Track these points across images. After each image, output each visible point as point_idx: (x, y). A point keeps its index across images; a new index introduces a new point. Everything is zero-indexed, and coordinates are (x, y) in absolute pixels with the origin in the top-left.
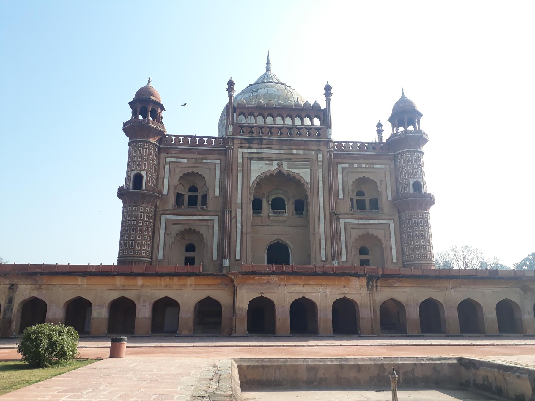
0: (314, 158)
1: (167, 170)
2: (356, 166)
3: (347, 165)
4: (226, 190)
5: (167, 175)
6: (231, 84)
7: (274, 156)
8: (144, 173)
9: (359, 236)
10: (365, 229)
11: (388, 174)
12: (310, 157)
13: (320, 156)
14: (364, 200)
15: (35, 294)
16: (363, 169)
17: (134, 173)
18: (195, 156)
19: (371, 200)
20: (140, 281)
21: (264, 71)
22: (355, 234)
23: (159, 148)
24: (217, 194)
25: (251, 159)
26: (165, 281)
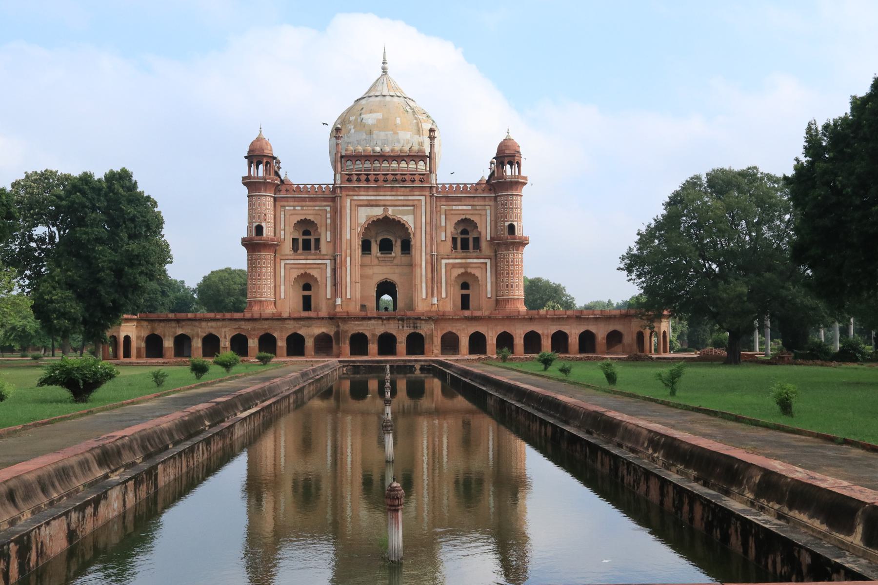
8: (263, 224)
21: (380, 72)
23: (275, 199)
24: (329, 239)
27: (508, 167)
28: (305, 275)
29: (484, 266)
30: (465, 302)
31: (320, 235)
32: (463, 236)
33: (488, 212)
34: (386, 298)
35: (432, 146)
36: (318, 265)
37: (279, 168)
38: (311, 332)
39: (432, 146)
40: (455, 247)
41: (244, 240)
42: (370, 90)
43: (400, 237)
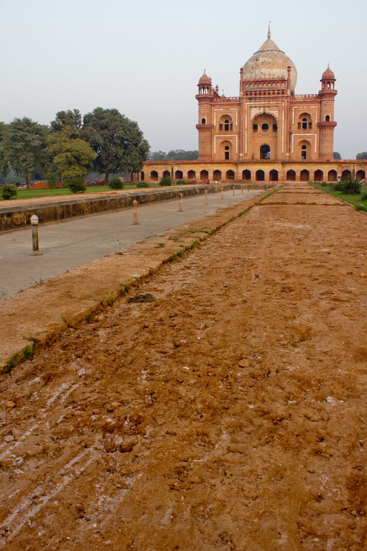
0: (280, 105)
1: (215, 115)
2: (301, 107)
3: (297, 107)
4: (240, 122)
5: (215, 117)
6: (242, 70)
7: (261, 105)
8: (206, 118)
11: (317, 111)
12: (278, 105)
13: (283, 104)
15: (179, 169)
16: (303, 109)
17: (202, 118)
18: (227, 107)
20: (209, 165)
22: (299, 140)
24: (237, 124)
25: (251, 107)
26: (216, 165)
36: (233, 137)
37: (217, 90)
39: (289, 74)
40: (299, 127)
41: (197, 126)
43: (272, 122)
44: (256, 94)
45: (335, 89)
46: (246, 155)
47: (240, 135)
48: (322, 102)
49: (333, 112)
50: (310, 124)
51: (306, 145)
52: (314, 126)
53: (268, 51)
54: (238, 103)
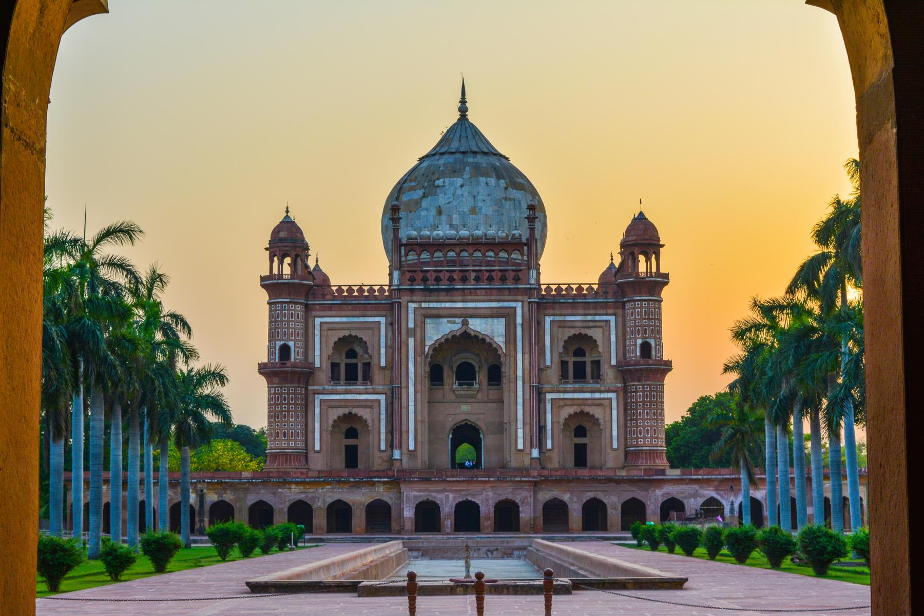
8: (291, 344)
9: (570, 416)
10: (577, 405)
14: (585, 362)
17: (279, 344)
19: (593, 362)
21: (455, 117)
24: (383, 364)
27: (642, 258)
28: (349, 417)
29: (607, 402)
30: (580, 456)
31: (371, 357)
32: (579, 359)
33: (613, 324)
34: (465, 448)
35: (532, 229)
38: (359, 498)
39: (532, 229)
40: (564, 376)
42: (440, 144)
44: (438, 280)
45: (662, 271)
46: (412, 454)
47: (395, 396)
48: (627, 306)
49: (660, 332)
50: (597, 364)
51: (587, 425)
52: (609, 374)
53: (464, 150)
54: (386, 303)
